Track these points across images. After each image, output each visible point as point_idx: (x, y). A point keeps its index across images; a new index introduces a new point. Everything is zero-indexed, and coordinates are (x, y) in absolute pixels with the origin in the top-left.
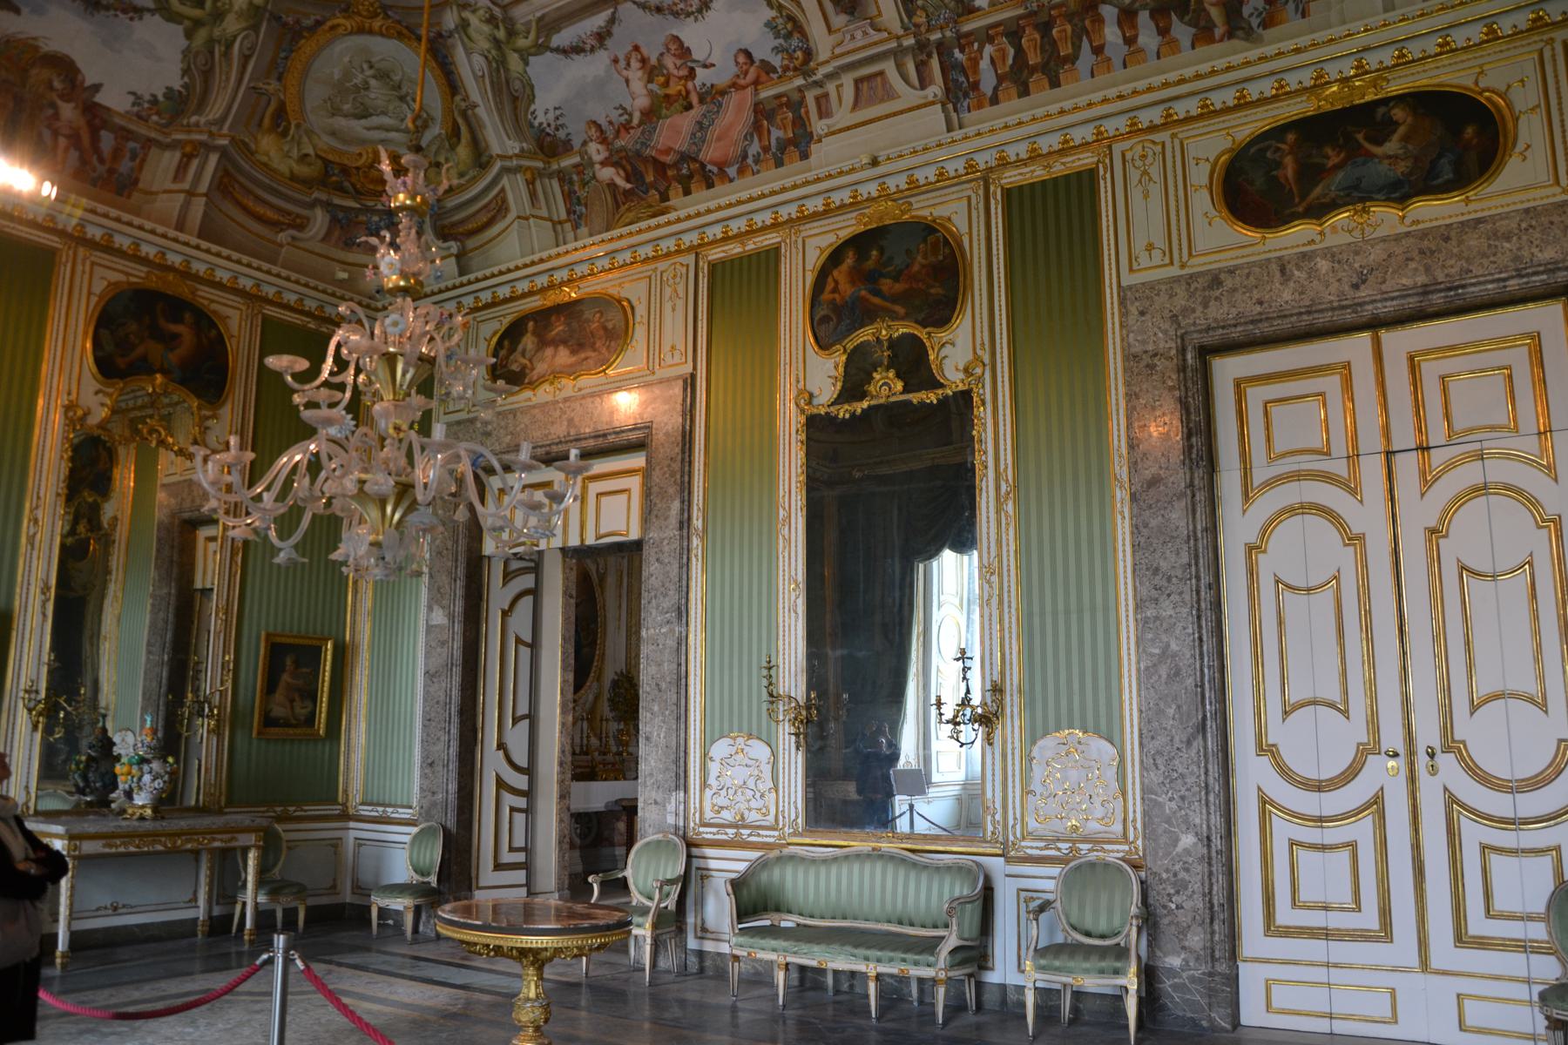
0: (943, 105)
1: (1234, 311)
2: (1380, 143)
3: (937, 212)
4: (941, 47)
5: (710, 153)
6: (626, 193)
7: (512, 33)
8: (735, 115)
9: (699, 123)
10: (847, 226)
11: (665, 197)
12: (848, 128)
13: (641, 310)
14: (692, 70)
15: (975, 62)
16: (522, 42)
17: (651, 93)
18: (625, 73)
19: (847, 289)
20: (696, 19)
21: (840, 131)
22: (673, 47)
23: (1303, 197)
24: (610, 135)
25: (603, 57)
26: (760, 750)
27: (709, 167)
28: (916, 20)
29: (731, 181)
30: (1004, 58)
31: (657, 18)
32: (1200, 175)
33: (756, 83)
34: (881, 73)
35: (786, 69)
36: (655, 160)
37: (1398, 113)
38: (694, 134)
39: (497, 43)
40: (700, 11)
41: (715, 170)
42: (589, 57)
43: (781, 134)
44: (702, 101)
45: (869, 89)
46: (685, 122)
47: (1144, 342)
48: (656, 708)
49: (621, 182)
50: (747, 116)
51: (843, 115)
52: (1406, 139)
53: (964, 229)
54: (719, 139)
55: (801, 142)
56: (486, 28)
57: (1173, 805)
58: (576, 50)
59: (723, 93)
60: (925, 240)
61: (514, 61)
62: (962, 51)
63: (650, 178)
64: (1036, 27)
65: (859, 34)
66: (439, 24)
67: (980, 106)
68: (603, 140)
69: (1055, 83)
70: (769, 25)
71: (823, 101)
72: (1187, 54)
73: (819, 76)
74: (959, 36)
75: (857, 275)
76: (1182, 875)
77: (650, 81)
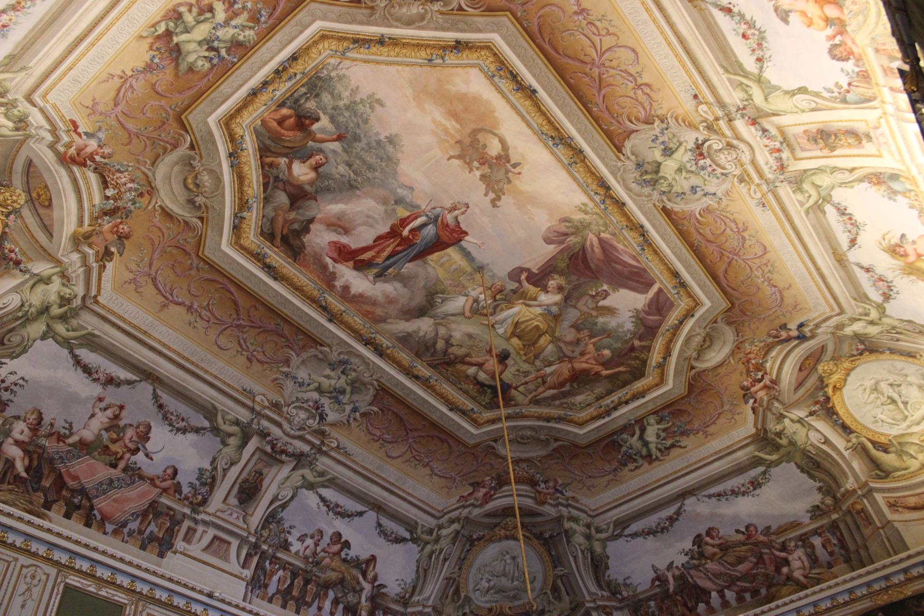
4: (264, 552)
5: (102, 504)
6: (17, 478)
7: (63, 318)
8: (136, 497)
9: (111, 481)
11: (48, 505)
12: (195, 559)
14: (138, 450)
15: (273, 573)
16: (60, 328)
17: (99, 437)
18: (97, 410)
20: (171, 431)
21: (190, 557)
22: (142, 428)
24: (44, 430)
25: (97, 390)
27: (96, 512)
28: (263, 532)
29: (105, 533)
30: (284, 582)
31: (155, 409)
33: (165, 490)
34: (229, 543)
35: (187, 498)
36: (60, 476)
38: (101, 484)
39: (45, 309)
40: (178, 430)
41: (99, 517)
42: (88, 381)
43: (156, 530)
44: (125, 470)
45: (217, 545)
46: (104, 472)
49: (20, 467)
50: (145, 503)
51: (195, 549)
54: (115, 501)
55: (164, 546)
56: (53, 298)
58: (87, 370)
59: (141, 478)
61: (38, 328)
62: (270, 564)
63: (46, 483)
64: (304, 578)
65: (235, 515)
66: (30, 259)
67: (263, 599)
68: (34, 429)
70: (201, 471)
71: (191, 532)
73: (199, 517)
74: (274, 556)
77: (107, 430)
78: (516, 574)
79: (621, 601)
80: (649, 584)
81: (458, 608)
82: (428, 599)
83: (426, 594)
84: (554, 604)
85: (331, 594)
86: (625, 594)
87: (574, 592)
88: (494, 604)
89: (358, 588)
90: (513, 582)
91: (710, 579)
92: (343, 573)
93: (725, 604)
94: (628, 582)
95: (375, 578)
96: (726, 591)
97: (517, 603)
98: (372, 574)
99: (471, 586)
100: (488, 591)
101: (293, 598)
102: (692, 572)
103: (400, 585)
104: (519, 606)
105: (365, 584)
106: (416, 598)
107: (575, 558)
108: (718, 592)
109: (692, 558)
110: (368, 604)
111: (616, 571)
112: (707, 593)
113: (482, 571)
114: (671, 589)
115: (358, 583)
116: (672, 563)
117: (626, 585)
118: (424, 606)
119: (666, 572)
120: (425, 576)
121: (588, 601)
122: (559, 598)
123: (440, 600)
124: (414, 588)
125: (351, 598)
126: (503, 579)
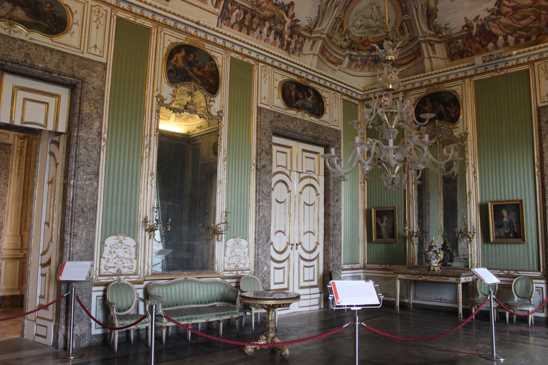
0: (218, 17)
1: (282, 126)
2: (308, 98)
3: (213, 53)
10: (181, 39)
13: (77, 17)
15: (232, 12)
19: (181, 64)
23: (295, 103)
26: (130, 241)
30: (240, 16)
32: (277, 84)
37: (311, 92)
47: (264, 125)
48: (81, 221)
52: (312, 99)
53: (221, 65)
57: (263, 259)
60: (209, 61)
62: (231, 6)
64: (251, 15)
67: (228, 26)
69: (248, 34)
72: (277, 48)
75: (185, 59)
76: (264, 278)
78: (379, 18)
79: (440, 38)
80: (461, 29)
81: (342, 36)
82: (324, 30)
83: (323, 27)
84: (399, 37)
85: (267, 24)
86: (444, 34)
87: (412, 29)
88: (363, 35)
89: (283, 21)
90: (376, 22)
91: (500, 29)
92: (274, 12)
93: (506, 44)
94: (448, 26)
95: (293, 16)
96: (509, 36)
97: (377, 35)
98: (291, 13)
99: (350, 24)
100: (360, 27)
101: (245, 26)
102: (490, 23)
103: (308, 20)
104: (377, 37)
105: (287, 19)
106: (317, 29)
107: (416, 9)
108: (504, 37)
109: (492, 14)
110: (289, 31)
111: (441, 20)
112: (496, 37)
113: (358, 15)
114: (474, 32)
115: (283, 18)
116: (478, 16)
117: (446, 29)
118: (322, 34)
119: (473, 22)
120: (323, 15)
121: (420, 37)
122: (403, 33)
123: (332, 30)
124: (316, 22)
125: (279, 27)
126: (370, 20)
